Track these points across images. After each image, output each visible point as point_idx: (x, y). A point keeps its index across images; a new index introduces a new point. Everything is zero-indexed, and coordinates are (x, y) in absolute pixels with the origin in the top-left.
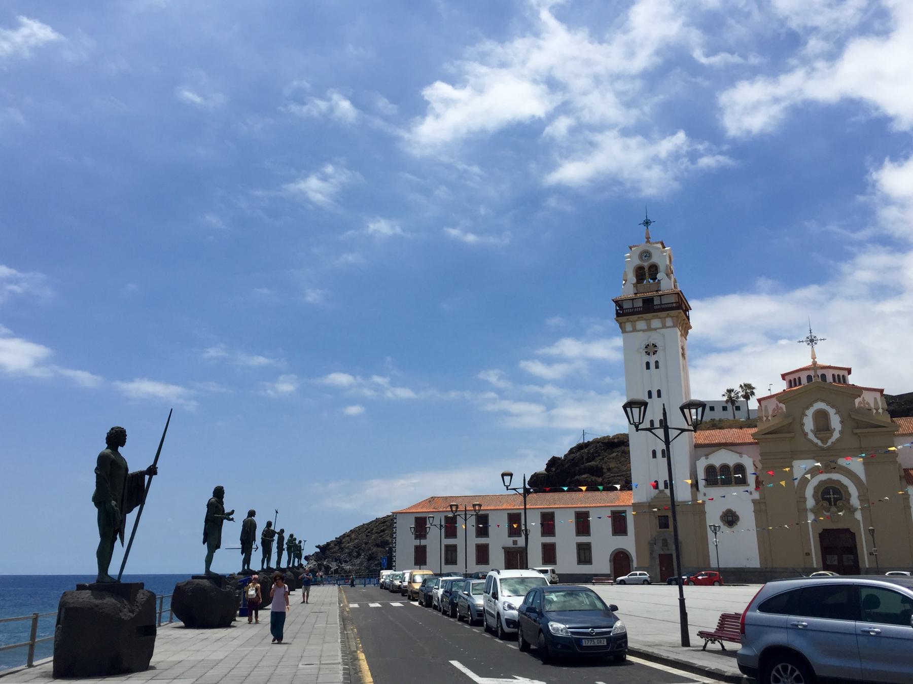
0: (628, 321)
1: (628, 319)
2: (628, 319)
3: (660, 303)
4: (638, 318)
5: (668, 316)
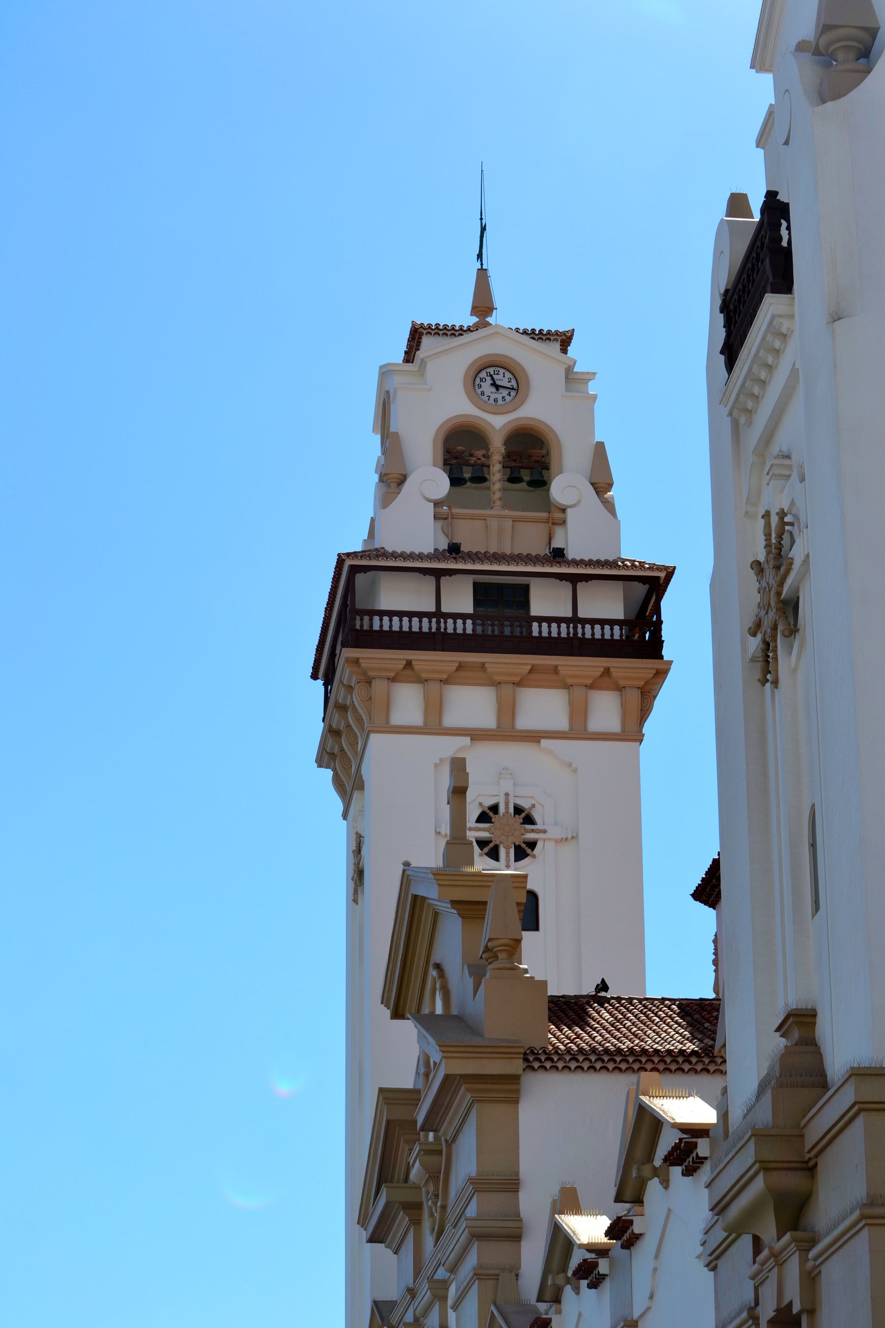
0: (408, 670)
1: (409, 664)
2: (409, 664)
3: (569, 614)
4: (461, 667)
5: (605, 680)
